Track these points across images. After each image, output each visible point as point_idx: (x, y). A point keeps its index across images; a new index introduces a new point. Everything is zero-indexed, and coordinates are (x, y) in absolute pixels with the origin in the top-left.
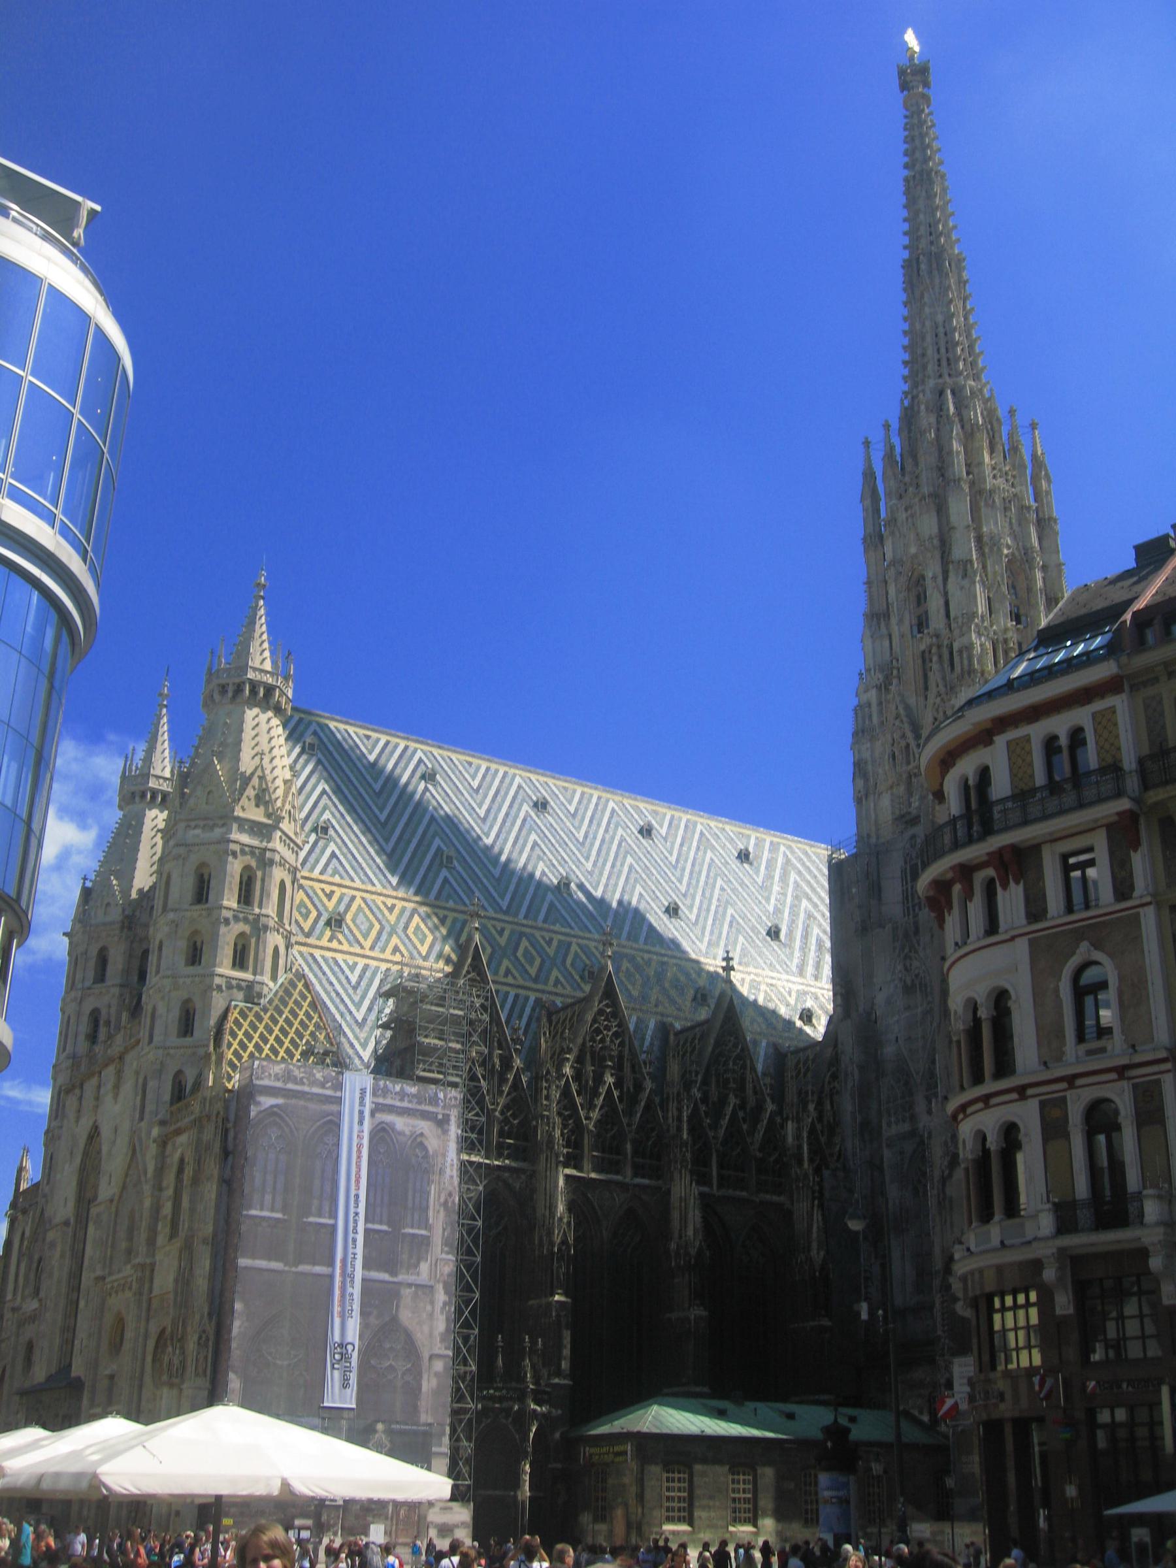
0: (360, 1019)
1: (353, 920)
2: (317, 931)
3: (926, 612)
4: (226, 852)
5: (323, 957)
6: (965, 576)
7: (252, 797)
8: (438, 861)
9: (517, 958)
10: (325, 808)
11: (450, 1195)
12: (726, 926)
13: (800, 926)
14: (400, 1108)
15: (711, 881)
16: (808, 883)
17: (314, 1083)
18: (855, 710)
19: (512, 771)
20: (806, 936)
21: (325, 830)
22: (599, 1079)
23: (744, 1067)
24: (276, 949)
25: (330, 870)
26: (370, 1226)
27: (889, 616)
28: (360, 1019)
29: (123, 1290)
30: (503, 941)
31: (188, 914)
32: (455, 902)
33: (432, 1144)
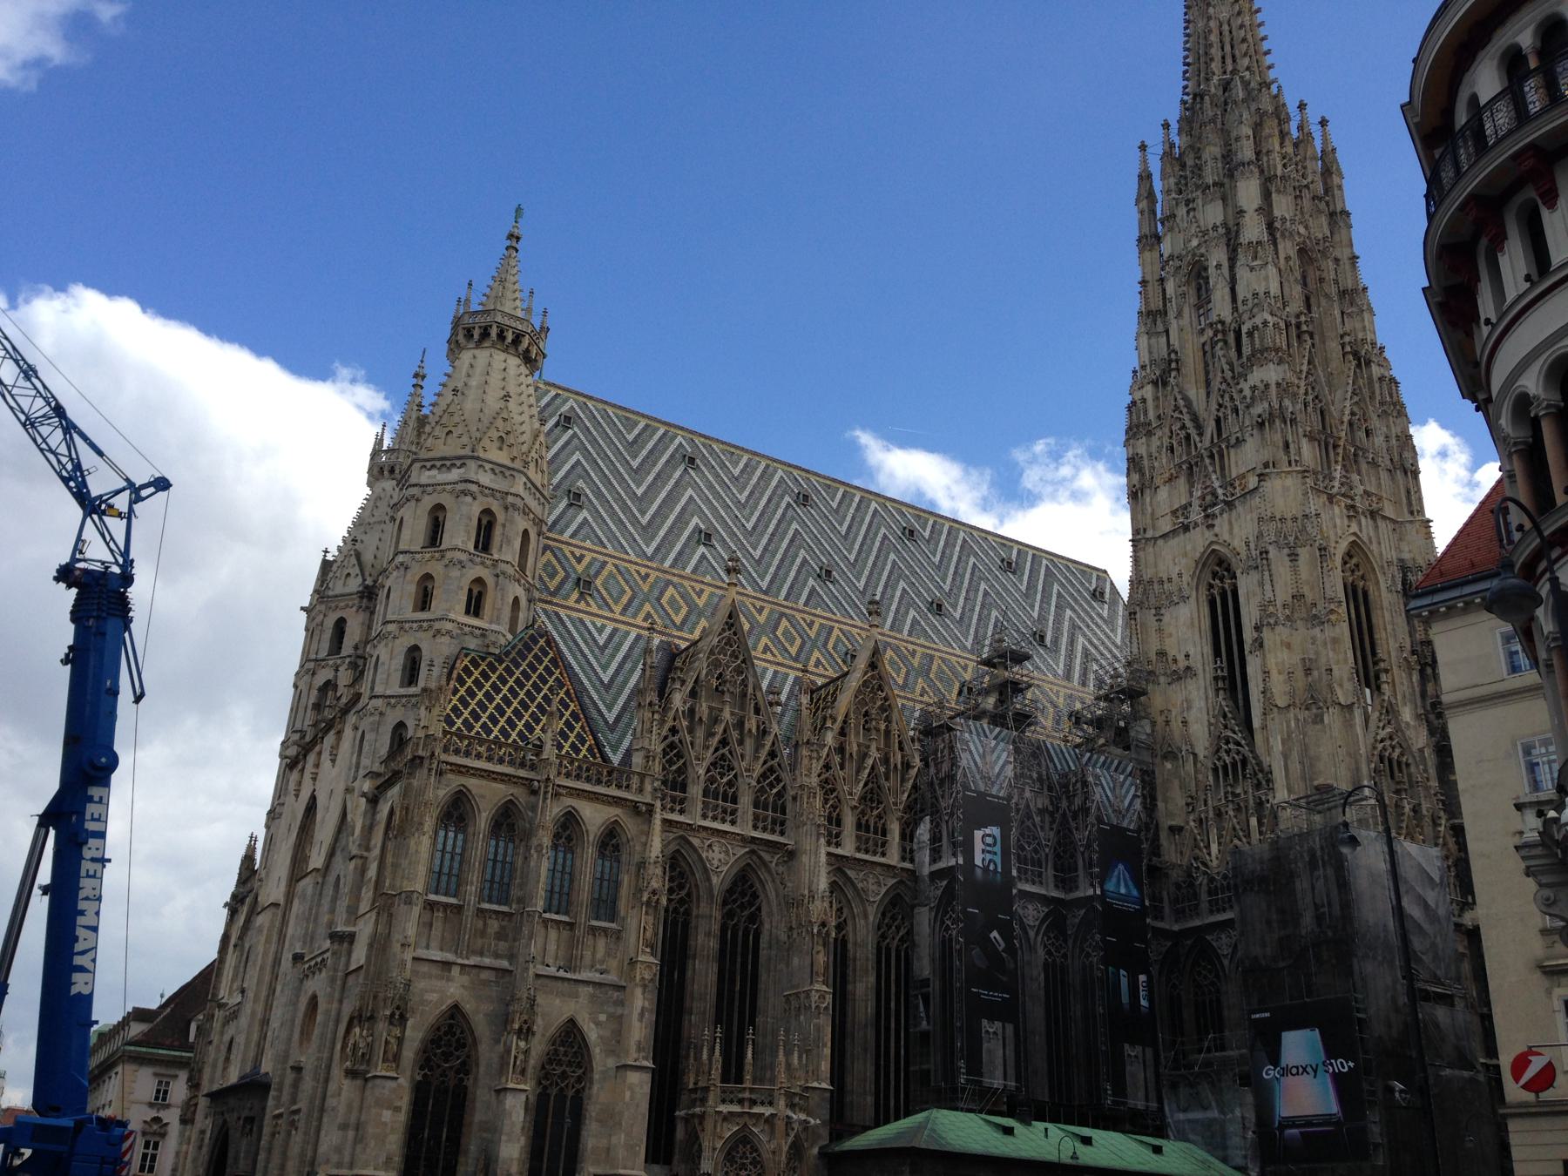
0: (606, 680)
2: (563, 592)
4: (465, 493)
5: (568, 616)
6: (1255, 258)
7: (495, 439)
10: (580, 477)
12: (991, 627)
13: (1065, 634)
16: (1072, 595)
18: (1129, 408)
20: (1072, 642)
21: (578, 496)
24: (516, 600)
28: (606, 680)
29: (320, 970)
30: (762, 619)
31: (418, 556)
32: (712, 577)
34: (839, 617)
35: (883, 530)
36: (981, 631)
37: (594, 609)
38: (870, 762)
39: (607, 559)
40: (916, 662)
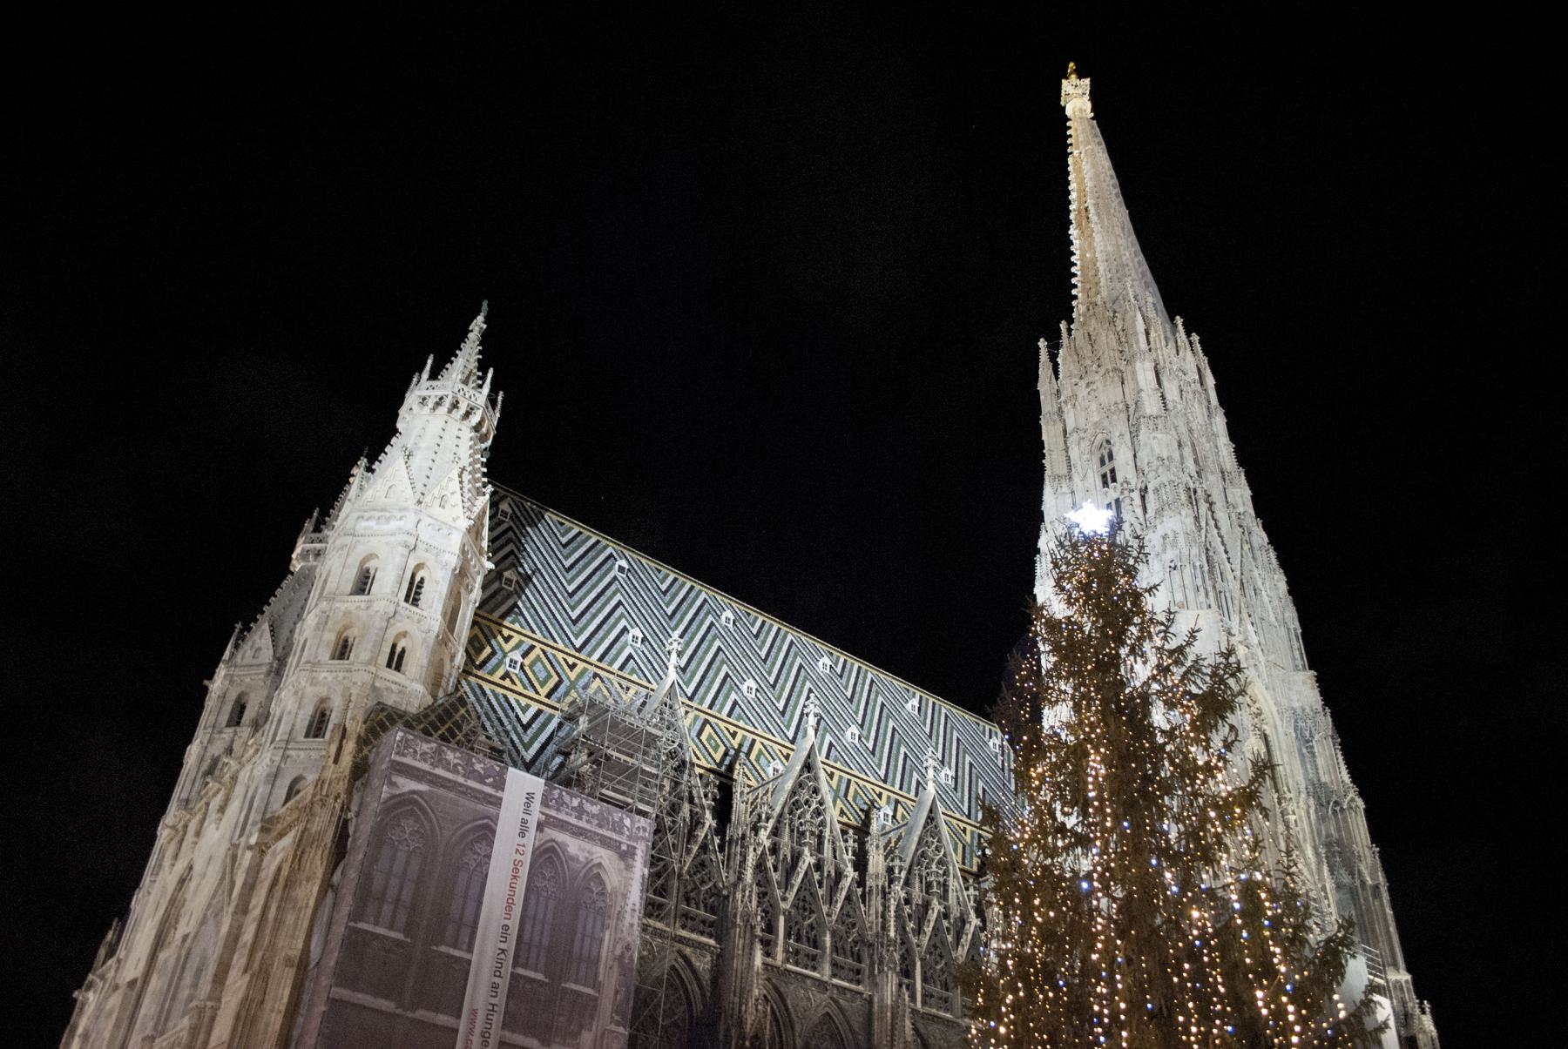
1: (531, 667)
2: (490, 666)
3: (1113, 471)
5: (493, 691)
8: (623, 639)
9: (702, 743)
11: (628, 948)
14: (573, 825)
15: (884, 720)
17: (470, 773)
19: (698, 587)
22: (797, 857)
23: (946, 873)
25: (510, 619)
26: (521, 971)
27: (1070, 478)
33: (612, 879)
34: (760, 732)
35: (799, 660)
36: (892, 763)
37: (519, 688)
38: (805, 867)
39: (535, 643)
40: (834, 783)
